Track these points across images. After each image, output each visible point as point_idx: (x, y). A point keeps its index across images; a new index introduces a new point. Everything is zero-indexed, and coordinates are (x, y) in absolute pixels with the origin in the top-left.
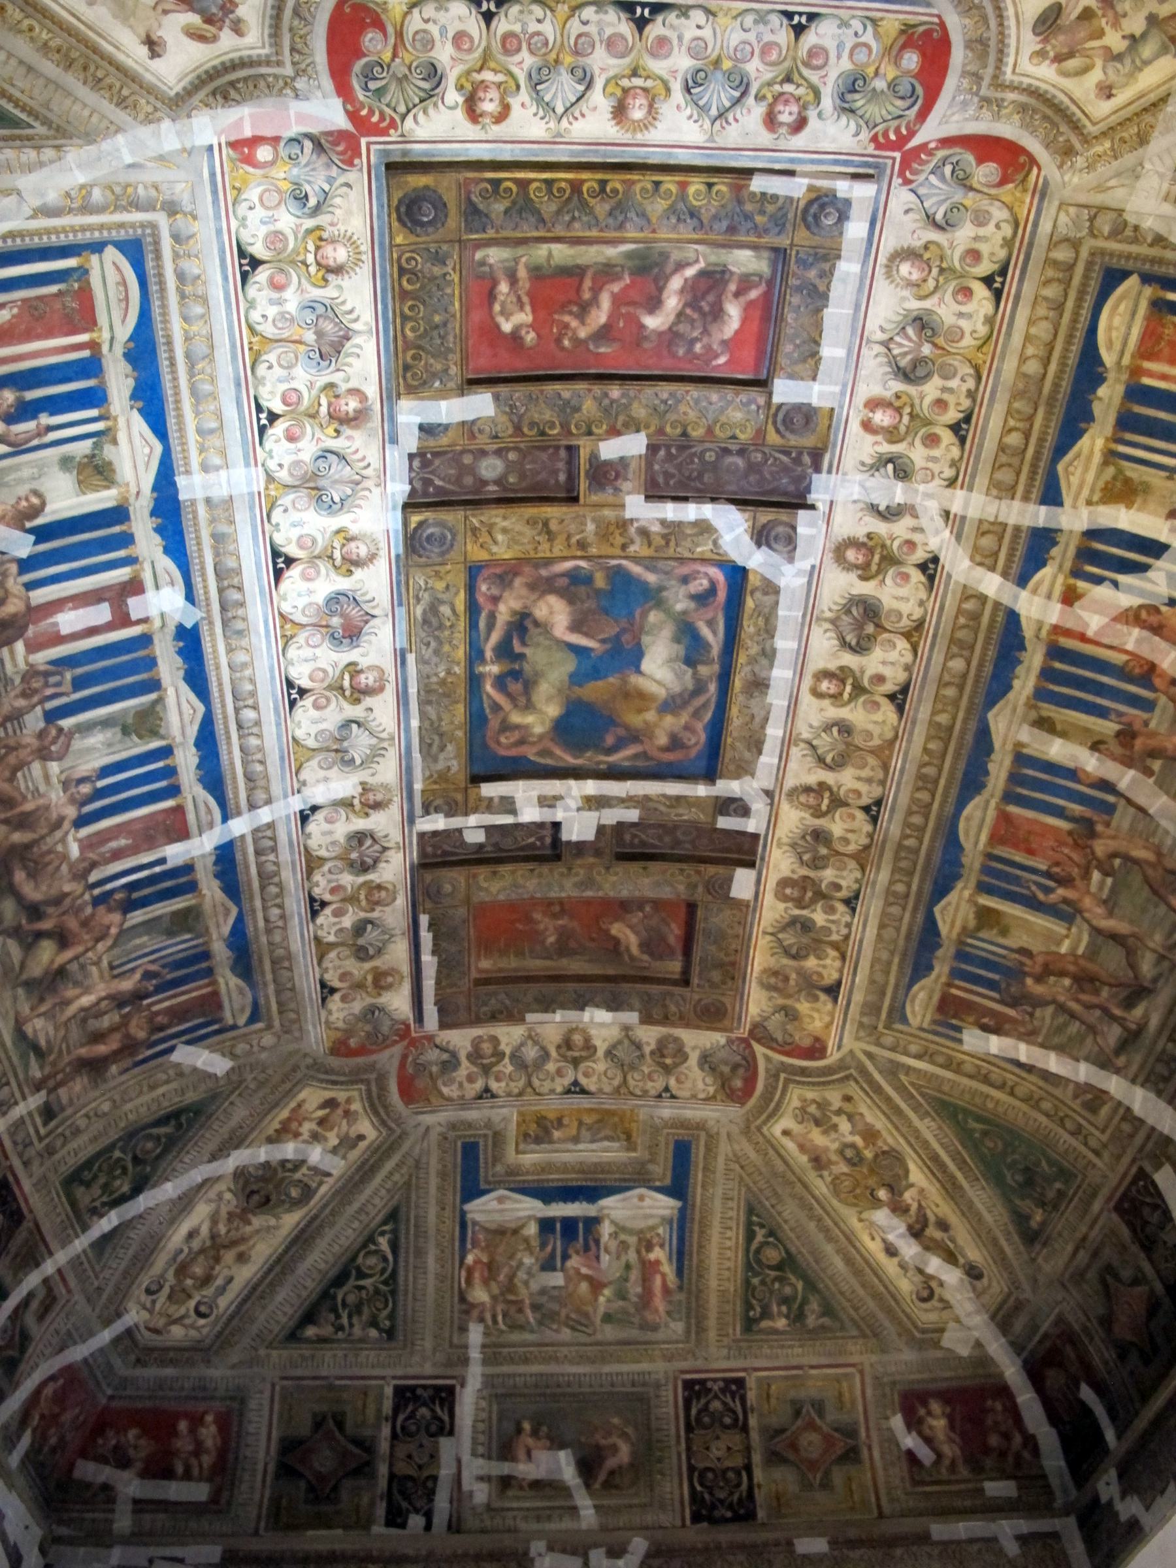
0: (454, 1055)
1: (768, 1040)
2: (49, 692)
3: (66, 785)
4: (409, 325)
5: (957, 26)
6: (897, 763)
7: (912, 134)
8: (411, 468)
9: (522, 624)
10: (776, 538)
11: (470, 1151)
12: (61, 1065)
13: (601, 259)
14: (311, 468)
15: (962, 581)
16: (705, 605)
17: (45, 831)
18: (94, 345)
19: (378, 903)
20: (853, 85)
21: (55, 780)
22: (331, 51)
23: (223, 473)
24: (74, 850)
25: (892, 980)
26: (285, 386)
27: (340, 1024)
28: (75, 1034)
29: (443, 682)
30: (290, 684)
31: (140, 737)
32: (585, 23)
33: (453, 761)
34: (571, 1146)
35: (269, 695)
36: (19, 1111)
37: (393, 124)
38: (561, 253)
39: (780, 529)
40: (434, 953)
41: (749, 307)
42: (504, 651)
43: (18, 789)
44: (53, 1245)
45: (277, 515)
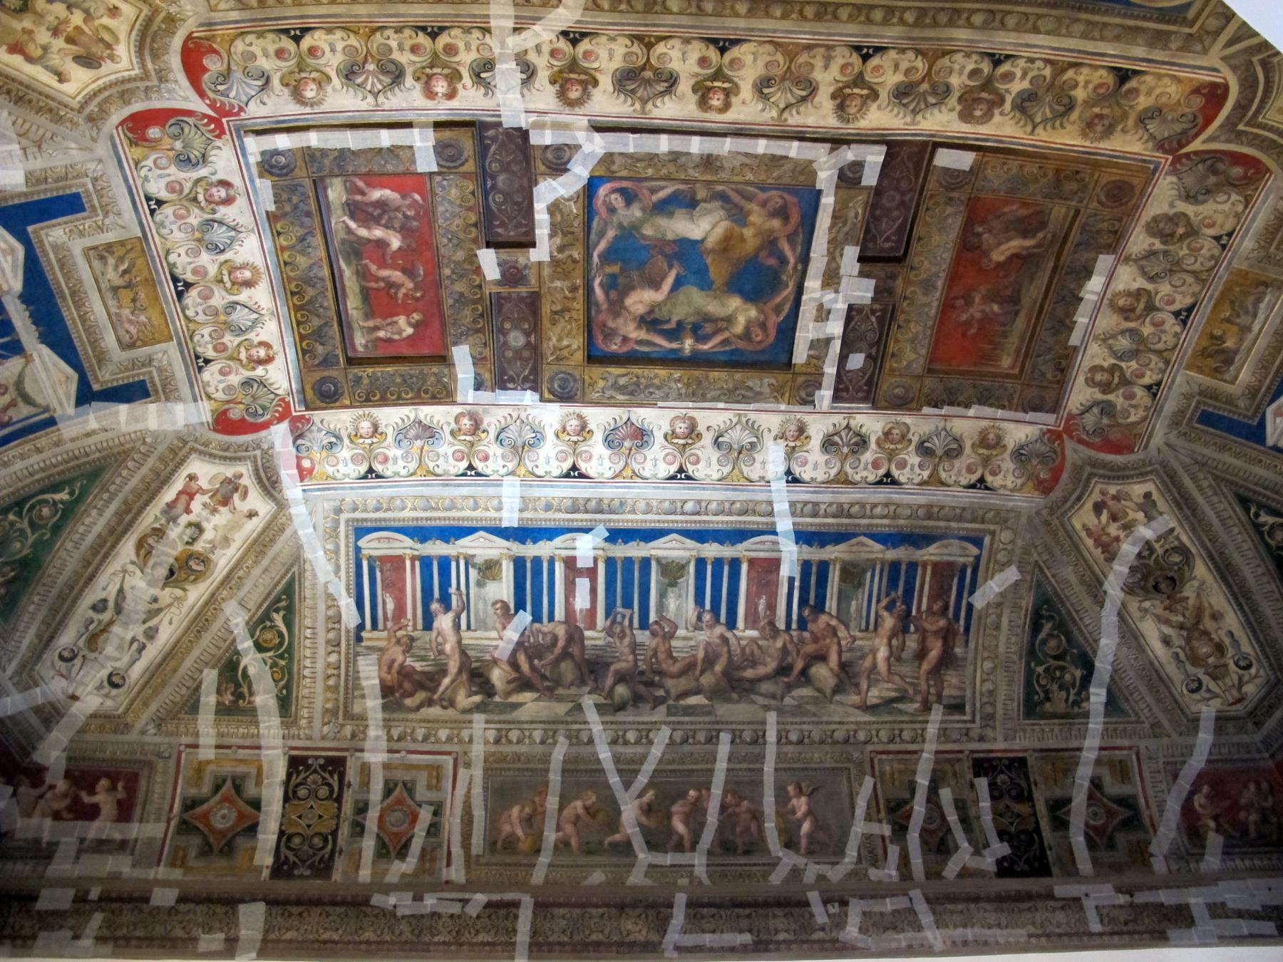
0: (1096, 403)
1: (1184, 138)
2: (626, 622)
3: (697, 628)
4: (404, 396)
5: (118, 115)
6: (804, 39)
7: (205, 116)
8: (515, 389)
9: (650, 321)
10: (559, 158)
11: (1207, 419)
12: (923, 686)
13: (354, 279)
14: (508, 449)
15: (580, 12)
16: (636, 196)
17: (725, 649)
18: (413, 559)
19: (903, 437)
20: (185, 161)
21: (691, 634)
22: (245, 433)
23: (504, 500)
24: (753, 633)
25: (1118, 20)
26: (451, 459)
27: (1019, 482)
28: (905, 669)
29: (688, 385)
30: (673, 478)
31: (682, 576)
32: (197, 313)
33: (763, 382)
34: (1250, 337)
35: (678, 491)
36: (932, 730)
37: (283, 400)
38: (353, 304)
39: (549, 155)
40: (967, 406)
41: (371, 185)
42: (675, 333)
43: (684, 658)
44: (1075, 744)
45: (539, 472)
